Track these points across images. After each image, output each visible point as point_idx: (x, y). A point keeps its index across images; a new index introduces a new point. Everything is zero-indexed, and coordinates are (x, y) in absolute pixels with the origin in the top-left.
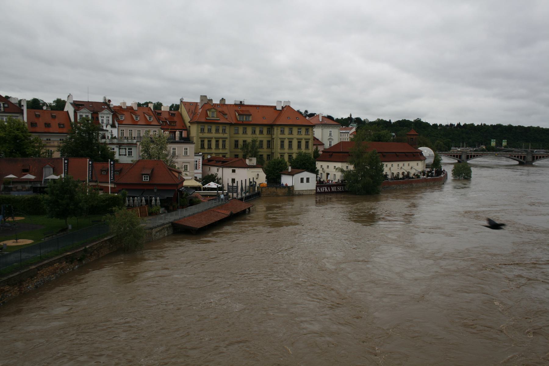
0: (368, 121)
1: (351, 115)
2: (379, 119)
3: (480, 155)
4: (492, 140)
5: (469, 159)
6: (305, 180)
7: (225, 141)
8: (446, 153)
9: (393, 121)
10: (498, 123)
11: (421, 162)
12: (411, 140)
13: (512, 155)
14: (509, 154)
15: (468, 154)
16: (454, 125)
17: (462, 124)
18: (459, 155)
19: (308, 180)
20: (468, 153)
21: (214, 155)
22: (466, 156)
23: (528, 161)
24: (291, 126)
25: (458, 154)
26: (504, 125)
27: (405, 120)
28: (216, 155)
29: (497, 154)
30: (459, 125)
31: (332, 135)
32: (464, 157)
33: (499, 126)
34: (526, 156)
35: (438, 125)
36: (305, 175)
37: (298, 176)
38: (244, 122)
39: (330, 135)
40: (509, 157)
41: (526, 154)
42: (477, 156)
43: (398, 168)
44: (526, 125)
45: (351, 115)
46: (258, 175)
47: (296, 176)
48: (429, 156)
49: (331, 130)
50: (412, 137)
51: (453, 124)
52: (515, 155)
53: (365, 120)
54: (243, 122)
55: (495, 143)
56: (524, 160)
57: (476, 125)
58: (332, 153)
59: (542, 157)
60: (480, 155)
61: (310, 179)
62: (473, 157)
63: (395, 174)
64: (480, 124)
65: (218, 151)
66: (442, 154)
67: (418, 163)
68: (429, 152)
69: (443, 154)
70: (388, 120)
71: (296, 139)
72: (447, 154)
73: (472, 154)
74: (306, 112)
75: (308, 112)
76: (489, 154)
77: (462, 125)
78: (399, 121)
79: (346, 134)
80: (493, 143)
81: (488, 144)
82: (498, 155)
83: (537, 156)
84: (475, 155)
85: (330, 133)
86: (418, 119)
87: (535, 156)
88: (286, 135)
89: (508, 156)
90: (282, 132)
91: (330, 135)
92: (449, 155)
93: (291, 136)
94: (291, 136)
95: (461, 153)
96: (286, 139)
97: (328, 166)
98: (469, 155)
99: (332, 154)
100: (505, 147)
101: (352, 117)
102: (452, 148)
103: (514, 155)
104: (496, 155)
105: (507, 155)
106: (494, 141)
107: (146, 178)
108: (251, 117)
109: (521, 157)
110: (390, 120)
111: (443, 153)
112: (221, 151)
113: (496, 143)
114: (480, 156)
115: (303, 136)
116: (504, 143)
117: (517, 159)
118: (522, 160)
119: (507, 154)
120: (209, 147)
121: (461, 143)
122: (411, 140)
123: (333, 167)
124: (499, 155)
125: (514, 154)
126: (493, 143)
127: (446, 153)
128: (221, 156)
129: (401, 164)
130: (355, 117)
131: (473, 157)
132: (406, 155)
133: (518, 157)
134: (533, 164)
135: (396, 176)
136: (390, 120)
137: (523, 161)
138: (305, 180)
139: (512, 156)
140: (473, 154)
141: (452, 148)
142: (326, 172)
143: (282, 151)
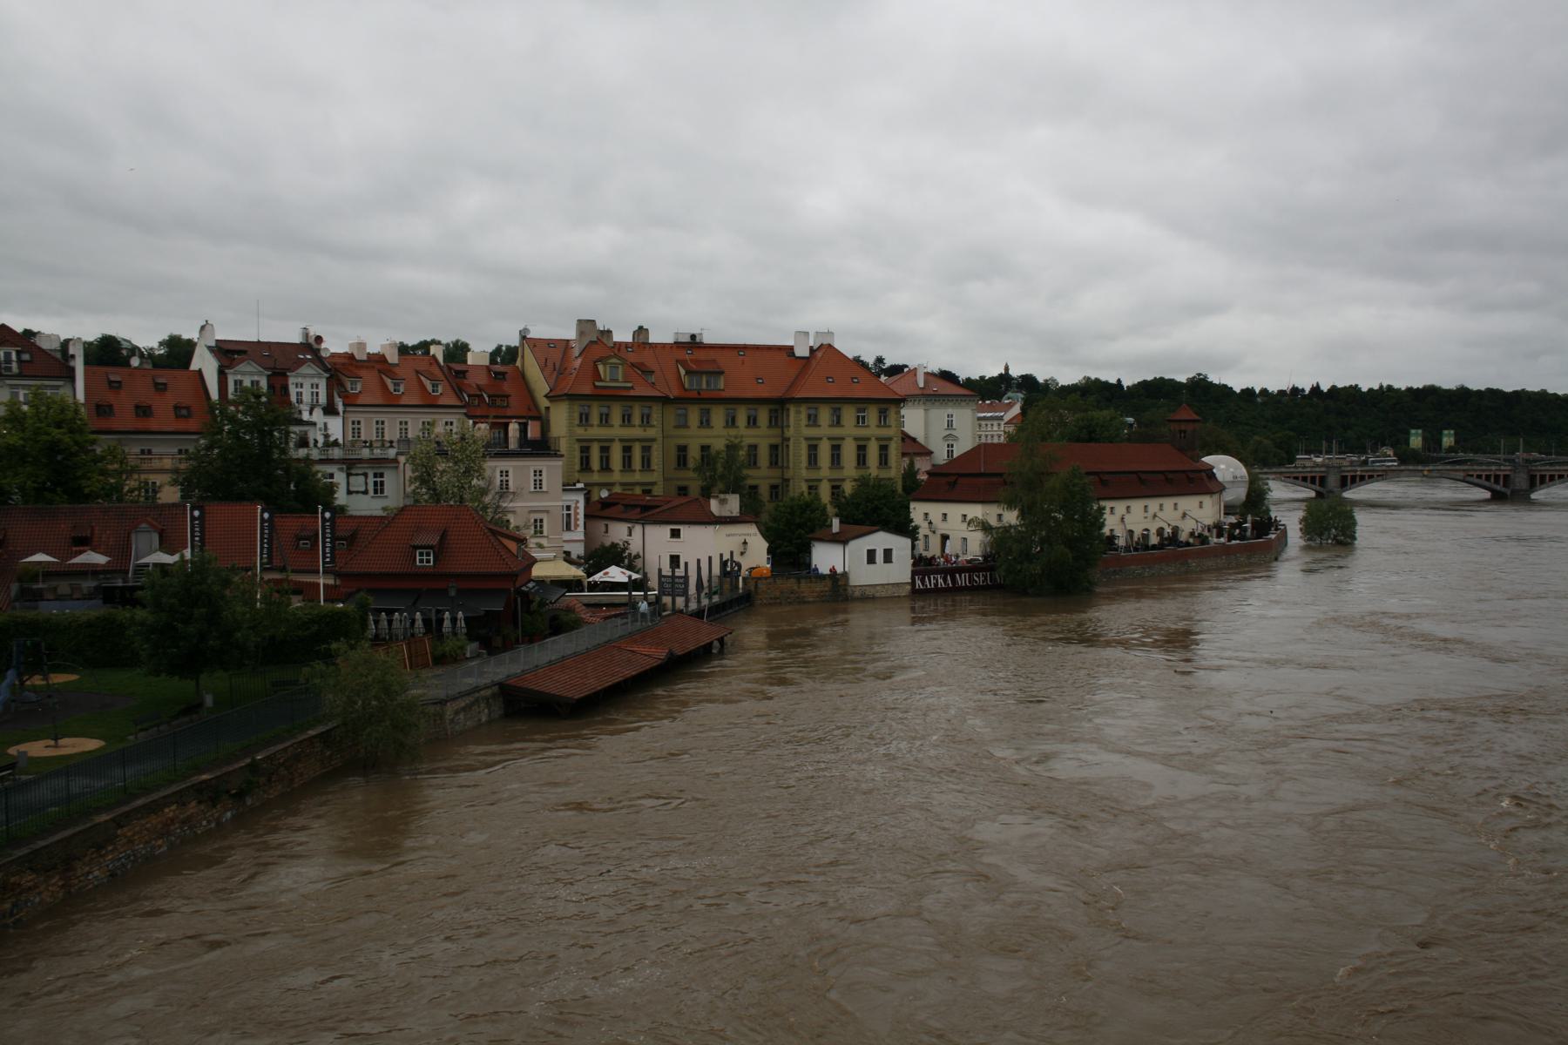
0: (1057, 384)
1: (1007, 368)
2: (1088, 379)
3: (1378, 476)
4: (1413, 431)
5: (1348, 488)
6: (880, 556)
7: (650, 447)
8: (1283, 470)
9: (1126, 383)
10: (1429, 383)
11: (1211, 497)
12: (1181, 437)
13: (1470, 473)
14: (1464, 470)
15: (1344, 471)
16: (1303, 390)
17: (1325, 388)
18: (1318, 475)
19: (888, 555)
20: (1343, 469)
21: (617, 489)
22: (1338, 477)
23: (1517, 488)
24: (836, 403)
25: (1316, 472)
26: (1446, 386)
27: (1162, 379)
28: (624, 490)
29: (1429, 471)
30: (1316, 390)
31: (954, 427)
32: (1333, 481)
33: (1431, 391)
35: (1257, 391)
36: (880, 540)
37: (861, 546)
38: (701, 393)
39: (950, 425)
40: (1461, 478)
41: (1510, 470)
42: (1371, 477)
43: (1146, 518)
44: (1508, 387)
45: (1007, 368)
46: (745, 543)
47: (853, 544)
48: (1232, 479)
49: (950, 411)
50: (1183, 427)
51: (1300, 388)
52: (1479, 473)
53: (1046, 381)
54: (699, 394)
55: (1420, 438)
56: (1505, 485)
57: (1365, 389)
58: (954, 478)
59: (1556, 477)
60: (1378, 476)
61: (894, 553)
62: (1358, 479)
63: (1138, 532)
64: (1376, 387)
65: (629, 478)
67: (1201, 502)
68: (1232, 470)
69: (1275, 473)
70: (1113, 381)
71: (851, 438)
73: (1357, 471)
74: (880, 360)
75: (885, 361)
77: (1325, 391)
78: (1145, 382)
79: (995, 423)
80: (1416, 441)
81: (1398, 441)
83: (1543, 473)
84: (1363, 474)
85: (948, 421)
86: (1199, 375)
87: (1538, 474)
88: (825, 429)
89: (1461, 475)
90: (813, 421)
91: (948, 426)
93: (837, 432)
94: (837, 432)
95: (1323, 469)
96: (825, 439)
97: (945, 515)
98: (1347, 476)
99: (957, 479)
100: (1450, 449)
101: (1011, 372)
102: (1298, 457)
103: (1475, 474)
104: (1426, 473)
105: (1458, 473)
106: (1417, 434)
107: (425, 558)
108: (722, 378)
109: (1497, 478)
110: (1119, 380)
111: (1274, 470)
112: (637, 477)
113: (1425, 439)
114: (1380, 478)
115: (872, 429)
116: (1448, 439)
117: (1487, 484)
118: (1498, 488)
119: (1457, 470)
120: (604, 466)
121: (1324, 442)
122: (1181, 437)
123: (960, 518)
124: (1434, 474)
125: (1476, 470)
126: (1416, 441)
127: (1283, 470)
128: (638, 491)
129: (1153, 504)
130: (1019, 375)
131: (1358, 479)
132: (1167, 479)
133: (1488, 478)
134: (1533, 496)
135: (1139, 539)
136: (1119, 380)
137: (1503, 490)
138: (880, 556)
139: (1472, 476)
140: (1358, 473)
141: (1298, 457)
142: (939, 532)
143: (813, 475)
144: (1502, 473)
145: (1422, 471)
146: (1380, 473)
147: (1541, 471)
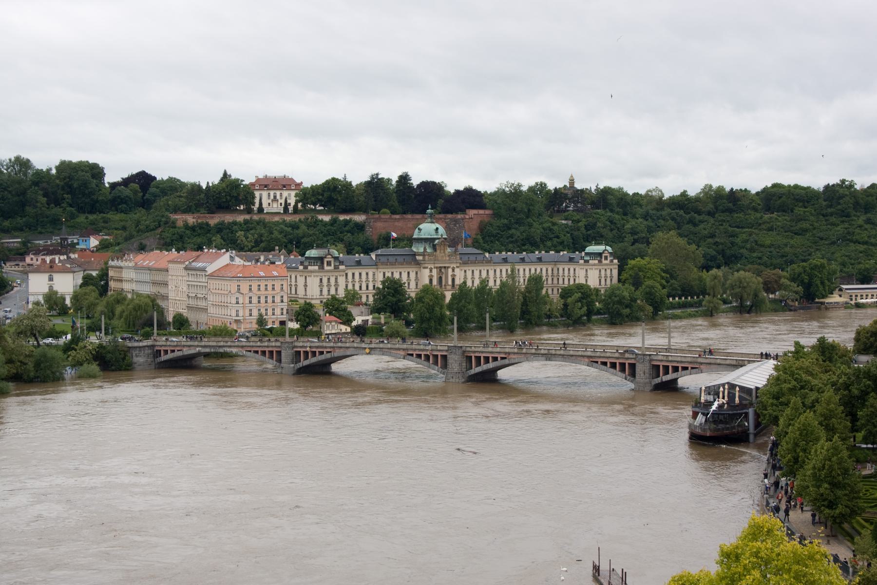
3: (328, 352)
14: (404, 350)
15: (297, 347)
18: (275, 349)
25: (272, 347)
34: (448, 356)
41: (447, 351)
60: (328, 352)
66: (234, 346)
72: (245, 346)
76: (351, 349)
82: (372, 352)
83: (477, 355)
87: (473, 355)
89: (402, 353)
92: (250, 351)
98: (300, 351)
103: (414, 353)
109: (436, 356)
140: (308, 349)
144: (439, 354)
145: (365, 348)
146: (329, 350)
147: (475, 352)
